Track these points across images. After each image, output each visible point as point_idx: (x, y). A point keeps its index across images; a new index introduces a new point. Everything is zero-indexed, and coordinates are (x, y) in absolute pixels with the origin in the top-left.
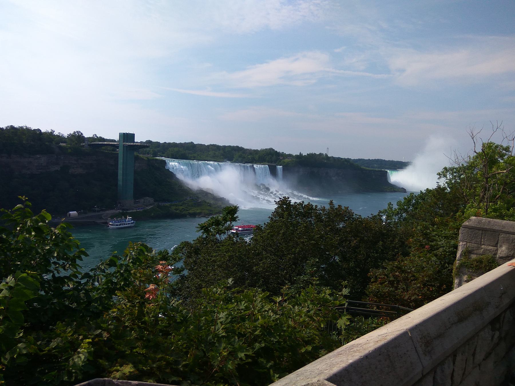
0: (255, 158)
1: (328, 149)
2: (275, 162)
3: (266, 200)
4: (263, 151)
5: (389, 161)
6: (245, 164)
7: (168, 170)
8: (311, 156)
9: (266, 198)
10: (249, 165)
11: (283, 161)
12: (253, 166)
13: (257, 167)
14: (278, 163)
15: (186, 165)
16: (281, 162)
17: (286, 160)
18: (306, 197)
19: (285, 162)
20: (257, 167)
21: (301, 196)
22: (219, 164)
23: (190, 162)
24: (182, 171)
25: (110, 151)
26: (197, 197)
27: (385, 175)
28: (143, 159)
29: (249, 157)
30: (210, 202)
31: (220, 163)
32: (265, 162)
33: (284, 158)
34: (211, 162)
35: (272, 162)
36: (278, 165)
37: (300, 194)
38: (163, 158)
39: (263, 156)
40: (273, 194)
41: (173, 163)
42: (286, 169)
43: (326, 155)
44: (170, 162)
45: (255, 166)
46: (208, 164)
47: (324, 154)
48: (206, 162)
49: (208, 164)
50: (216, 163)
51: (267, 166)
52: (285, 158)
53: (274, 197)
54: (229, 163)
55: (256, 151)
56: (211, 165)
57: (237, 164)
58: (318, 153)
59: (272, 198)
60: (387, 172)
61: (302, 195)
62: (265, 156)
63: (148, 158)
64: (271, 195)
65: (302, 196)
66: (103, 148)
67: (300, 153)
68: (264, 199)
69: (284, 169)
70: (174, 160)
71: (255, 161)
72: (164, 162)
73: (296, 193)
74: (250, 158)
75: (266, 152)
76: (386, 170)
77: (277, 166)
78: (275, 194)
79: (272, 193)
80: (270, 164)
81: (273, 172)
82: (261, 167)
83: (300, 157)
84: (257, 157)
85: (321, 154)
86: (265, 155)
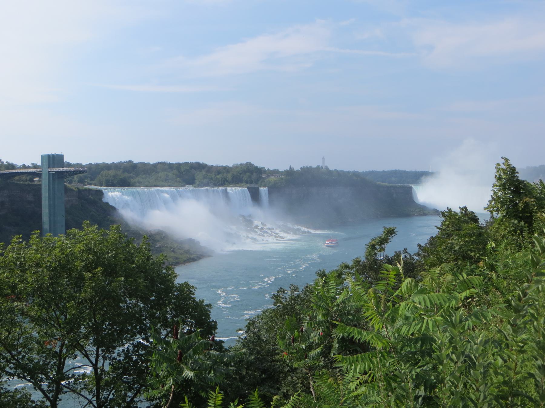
0: (227, 179)
1: (324, 158)
2: (257, 182)
3: (250, 238)
4: (236, 167)
5: (411, 172)
6: (213, 187)
7: (107, 204)
8: (306, 171)
9: (250, 236)
10: (220, 188)
11: (267, 180)
12: (226, 189)
13: (232, 191)
14: (261, 184)
15: (133, 194)
16: (264, 181)
17: (272, 179)
18: (306, 230)
19: (270, 182)
20: (232, 191)
21: (299, 230)
22: (177, 190)
23: (138, 190)
24: (126, 205)
25: (26, 181)
26: (153, 240)
27: (409, 191)
28: (72, 190)
29: (218, 177)
30: (172, 246)
31: (180, 189)
32: (242, 183)
33: (268, 176)
34: (167, 189)
35: (251, 183)
36: (261, 187)
37: (297, 227)
38: (100, 188)
39: (239, 174)
40: (258, 229)
41: (113, 194)
42: (273, 189)
43: (327, 168)
44: (109, 192)
45: (229, 190)
46: (163, 192)
47: (323, 167)
48: (159, 188)
49: (163, 192)
50: (172, 189)
51: (246, 188)
52: (269, 176)
53: (261, 233)
54: (190, 188)
55: (226, 169)
56: (167, 192)
57: (202, 188)
58: (314, 166)
59: (259, 235)
60: (411, 188)
61: (300, 227)
62: (241, 174)
63: (78, 188)
64: (257, 230)
65: (300, 229)
66: (17, 178)
67: (290, 168)
68: (248, 237)
69: (270, 193)
70: (115, 189)
71: (227, 183)
72: (100, 193)
73: (290, 225)
74: (219, 179)
75: (241, 168)
76: (410, 185)
77: (260, 188)
78: (262, 228)
79: (257, 227)
80: (249, 185)
81: (255, 196)
82: (238, 190)
83: (290, 173)
84: (229, 176)
85: (319, 168)
86: (241, 172)
